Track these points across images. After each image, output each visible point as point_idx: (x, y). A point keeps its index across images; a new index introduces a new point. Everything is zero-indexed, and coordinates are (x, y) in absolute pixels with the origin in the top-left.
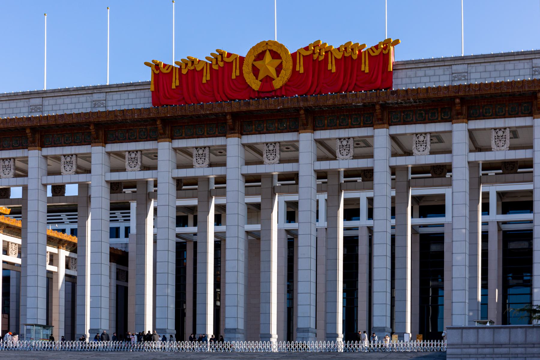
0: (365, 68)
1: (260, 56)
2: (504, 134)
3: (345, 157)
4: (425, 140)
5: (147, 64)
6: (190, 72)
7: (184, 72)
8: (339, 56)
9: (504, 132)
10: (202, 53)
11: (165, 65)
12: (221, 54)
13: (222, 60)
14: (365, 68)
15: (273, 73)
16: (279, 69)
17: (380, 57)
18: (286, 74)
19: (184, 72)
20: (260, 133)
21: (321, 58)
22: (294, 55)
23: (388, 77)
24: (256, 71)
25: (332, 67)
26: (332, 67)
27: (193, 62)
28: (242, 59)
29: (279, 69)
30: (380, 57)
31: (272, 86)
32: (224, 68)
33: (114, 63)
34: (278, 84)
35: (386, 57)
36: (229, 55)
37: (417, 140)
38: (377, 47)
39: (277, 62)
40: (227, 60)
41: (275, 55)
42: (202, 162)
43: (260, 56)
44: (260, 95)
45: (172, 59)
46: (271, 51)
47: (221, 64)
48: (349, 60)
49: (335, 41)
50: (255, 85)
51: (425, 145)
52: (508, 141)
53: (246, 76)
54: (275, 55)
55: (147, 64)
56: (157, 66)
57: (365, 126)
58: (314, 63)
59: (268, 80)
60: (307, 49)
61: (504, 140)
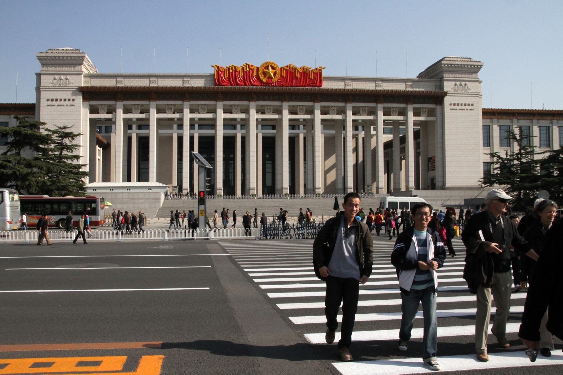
0: (312, 77)
1: (267, 68)
5: (212, 66)
6: (233, 72)
7: (231, 71)
8: (301, 71)
10: (239, 64)
11: (221, 68)
12: (247, 64)
13: (249, 68)
14: (312, 77)
17: (318, 73)
18: (278, 76)
20: (264, 100)
22: (281, 69)
23: (321, 82)
24: (265, 74)
27: (235, 67)
28: (258, 68)
29: (275, 74)
30: (318, 73)
32: (248, 71)
33: (195, 64)
34: (275, 80)
35: (321, 74)
36: (252, 66)
38: (316, 69)
39: (274, 71)
41: (273, 68)
44: (267, 84)
45: (224, 65)
48: (305, 73)
49: (299, 64)
53: (260, 76)
55: (212, 66)
56: (218, 67)
57: (310, 101)
58: (290, 73)
59: (270, 78)
60: (287, 66)
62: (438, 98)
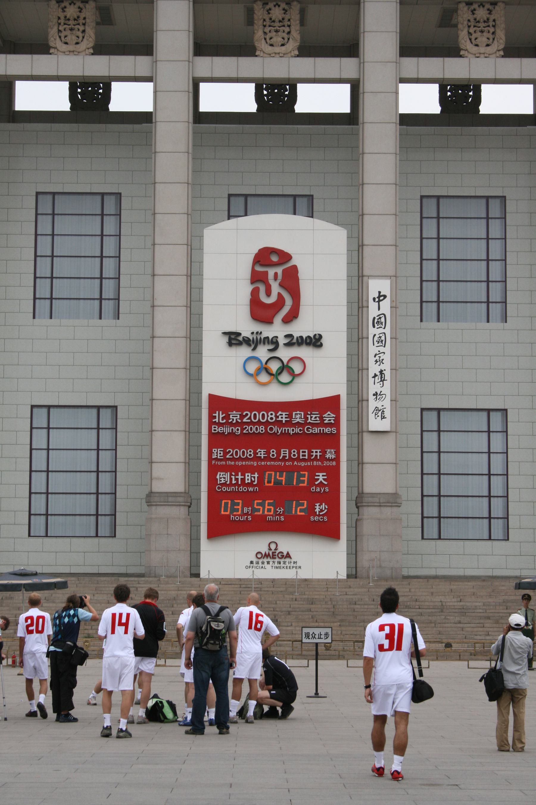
2: (492, 17)
3: (482, 49)
4: (287, 17)
9: (490, 12)
37: (267, 17)
42: (75, 40)
51: (287, 29)
52: (90, 32)
61: (492, 30)
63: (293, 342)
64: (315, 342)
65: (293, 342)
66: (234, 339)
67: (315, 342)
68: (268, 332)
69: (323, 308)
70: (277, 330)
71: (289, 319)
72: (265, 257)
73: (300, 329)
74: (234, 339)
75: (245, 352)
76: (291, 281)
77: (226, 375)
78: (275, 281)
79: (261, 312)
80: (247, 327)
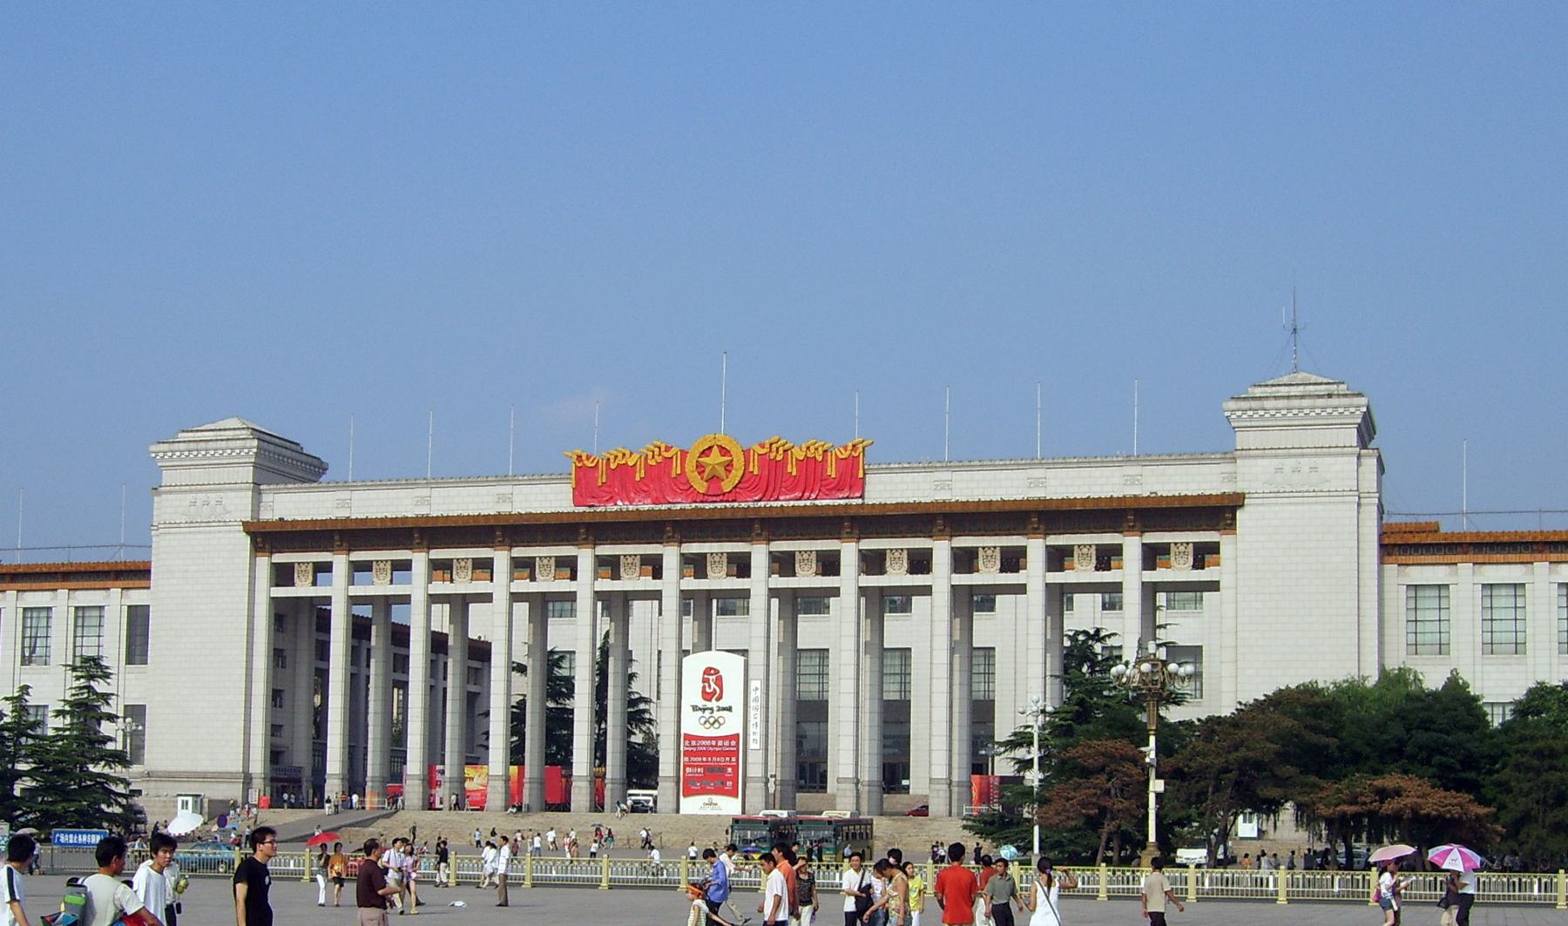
1: (706, 452)
14: (832, 472)
15: (721, 471)
16: (729, 467)
18: (737, 474)
19: (613, 466)
21: (779, 458)
24: (700, 468)
25: (792, 469)
26: (792, 469)
31: (720, 488)
34: (727, 486)
40: (668, 455)
41: (724, 451)
43: (706, 452)
46: (721, 448)
47: (659, 459)
50: (701, 486)
53: (689, 474)
54: (724, 451)
59: (714, 479)
62: (1218, 513)
63: (719, 709)
64: (729, 709)
65: (719, 709)
66: (695, 708)
67: (729, 709)
68: (709, 705)
69: (732, 693)
70: (713, 704)
71: (719, 699)
72: (708, 671)
73: (722, 703)
74: (695, 708)
75: (700, 713)
76: (719, 681)
77: (692, 724)
78: (713, 681)
79: (707, 696)
80: (701, 703)
